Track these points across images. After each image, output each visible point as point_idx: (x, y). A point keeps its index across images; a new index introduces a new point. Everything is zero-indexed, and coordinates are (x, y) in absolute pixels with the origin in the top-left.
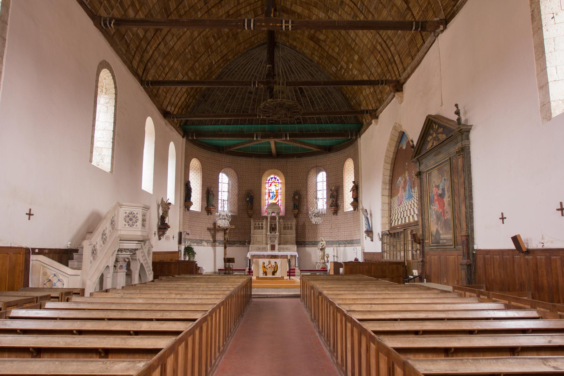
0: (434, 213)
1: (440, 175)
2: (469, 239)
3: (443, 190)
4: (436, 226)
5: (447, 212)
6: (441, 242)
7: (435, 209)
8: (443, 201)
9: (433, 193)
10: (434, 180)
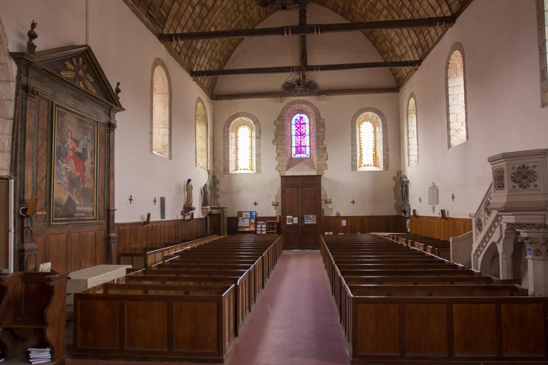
0: (64, 173)
1: (81, 130)
2: (109, 213)
3: (84, 150)
4: (68, 193)
5: (88, 180)
6: (76, 215)
7: (66, 168)
8: (83, 165)
9: (66, 145)
10: (70, 128)
